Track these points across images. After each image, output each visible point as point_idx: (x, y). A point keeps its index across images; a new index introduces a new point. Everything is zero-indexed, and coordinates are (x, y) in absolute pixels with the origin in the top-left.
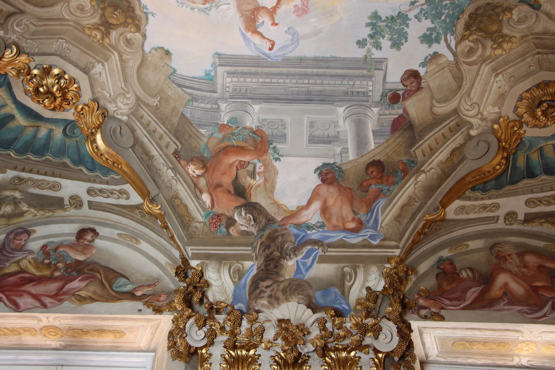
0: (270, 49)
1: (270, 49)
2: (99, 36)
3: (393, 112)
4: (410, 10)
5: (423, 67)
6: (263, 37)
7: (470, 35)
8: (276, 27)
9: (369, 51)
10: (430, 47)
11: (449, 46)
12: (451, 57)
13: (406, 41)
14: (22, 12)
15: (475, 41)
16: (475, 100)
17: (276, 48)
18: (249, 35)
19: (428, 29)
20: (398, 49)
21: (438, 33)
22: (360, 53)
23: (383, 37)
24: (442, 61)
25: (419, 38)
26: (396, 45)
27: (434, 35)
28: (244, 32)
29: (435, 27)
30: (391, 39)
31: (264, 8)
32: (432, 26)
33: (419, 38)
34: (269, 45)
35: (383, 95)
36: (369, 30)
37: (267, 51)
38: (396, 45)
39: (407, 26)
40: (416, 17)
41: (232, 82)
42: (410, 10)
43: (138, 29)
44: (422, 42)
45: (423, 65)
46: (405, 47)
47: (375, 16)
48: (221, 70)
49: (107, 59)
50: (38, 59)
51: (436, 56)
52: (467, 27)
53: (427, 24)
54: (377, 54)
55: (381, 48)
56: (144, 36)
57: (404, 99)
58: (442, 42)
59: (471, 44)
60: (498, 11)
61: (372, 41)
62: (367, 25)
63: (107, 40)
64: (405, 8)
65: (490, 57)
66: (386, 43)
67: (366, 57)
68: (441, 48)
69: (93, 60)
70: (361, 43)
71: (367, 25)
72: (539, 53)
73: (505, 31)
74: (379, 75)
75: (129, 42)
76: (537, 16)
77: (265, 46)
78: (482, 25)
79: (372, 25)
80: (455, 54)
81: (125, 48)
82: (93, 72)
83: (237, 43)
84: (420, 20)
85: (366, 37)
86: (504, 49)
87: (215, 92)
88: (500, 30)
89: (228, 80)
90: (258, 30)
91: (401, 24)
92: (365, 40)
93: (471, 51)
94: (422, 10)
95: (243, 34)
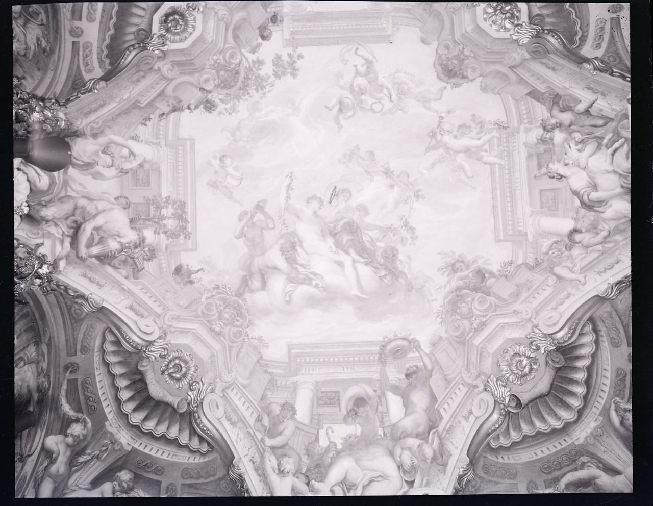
0: (357, 49)
1: (357, 49)
2: (466, 50)
3: (274, 10)
4: (274, 81)
5: (259, 43)
6: (362, 56)
7: (235, 68)
8: (355, 64)
9: (295, 52)
10: (258, 57)
11: (247, 59)
12: (243, 51)
13: (273, 60)
14: (511, 67)
15: (231, 64)
16: (222, 22)
17: (354, 49)
18: (371, 58)
19: (261, 69)
20: (277, 55)
21: (254, 67)
22: (300, 50)
23: (287, 62)
24: (249, 49)
25: (265, 63)
26: (278, 57)
27: (256, 66)
28: (374, 60)
29: (257, 71)
30: (283, 61)
31: (362, 76)
32: (259, 72)
33: (265, 63)
34: (359, 52)
35: (282, 21)
36: (297, 65)
37: (360, 48)
38: (278, 57)
39: (274, 71)
40: (270, 77)
41: (382, 24)
42: (274, 81)
43: (439, 56)
44: (263, 60)
45: (259, 45)
46: (273, 56)
47: (294, 76)
48: (389, 32)
49: (463, 35)
50: (507, 35)
51: (253, 51)
52: (237, 73)
53: (262, 73)
54: (290, 50)
55: (288, 54)
56: (437, 52)
57: (268, 19)
58: (251, 62)
59: (233, 61)
60: (223, 85)
61: (294, 59)
62: (298, 70)
63: (461, 48)
64: (277, 82)
65: (220, 53)
66: (285, 58)
67: (297, 48)
68: (252, 57)
69: (471, 34)
70: (300, 57)
71: (298, 70)
72: (191, 60)
73: (214, 72)
74: (287, 36)
75: (447, 47)
76: (199, 83)
77: (362, 51)
78: (230, 74)
79: (294, 69)
80: (242, 54)
81: (450, 43)
82: (473, 26)
83: (380, 52)
84: (267, 74)
85: (298, 61)
86: (213, 60)
87: (393, 16)
88: (218, 72)
89: (384, 26)
90: (365, 61)
91: (278, 71)
92: (298, 59)
93: (232, 56)
94: (267, 82)
95: (375, 58)
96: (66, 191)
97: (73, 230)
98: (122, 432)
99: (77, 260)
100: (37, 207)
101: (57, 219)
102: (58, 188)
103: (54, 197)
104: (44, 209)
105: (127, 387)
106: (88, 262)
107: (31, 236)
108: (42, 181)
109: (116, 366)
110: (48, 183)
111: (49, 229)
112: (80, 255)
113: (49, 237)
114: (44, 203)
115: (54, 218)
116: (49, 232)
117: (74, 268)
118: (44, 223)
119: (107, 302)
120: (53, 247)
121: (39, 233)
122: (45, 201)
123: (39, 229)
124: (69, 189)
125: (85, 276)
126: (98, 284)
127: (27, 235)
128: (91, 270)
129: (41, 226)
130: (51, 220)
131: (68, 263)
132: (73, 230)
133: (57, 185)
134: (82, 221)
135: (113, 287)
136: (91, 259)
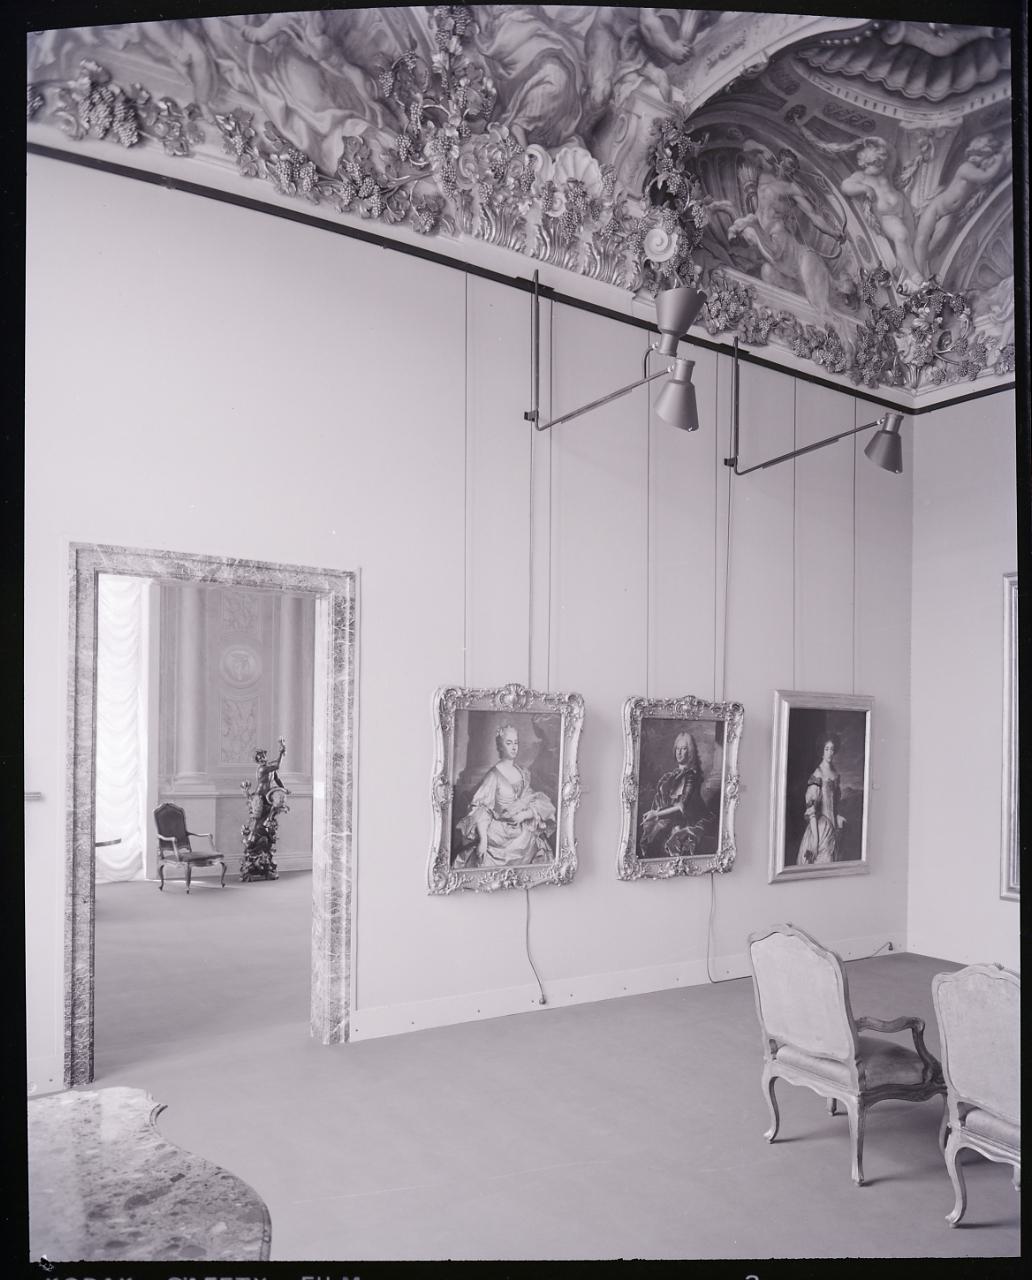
96: (577, 35)
97: (640, 52)
98: (933, 117)
99: (684, 66)
100: (588, 106)
101: (614, 75)
102: (571, 52)
103: (581, 65)
104: (593, 92)
105: (891, 72)
106: (697, 48)
107: (621, 137)
108: (552, 81)
109: (851, 65)
110: (557, 67)
111: (623, 97)
112: (681, 58)
113: (634, 103)
114: (584, 90)
115: (610, 79)
116: (627, 99)
117: (692, 78)
118: (611, 102)
119: (769, 46)
120: (648, 99)
121: (623, 119)
122: (582, 86)
123: (617, 116)
124: (576, 28)
125: (712, 64)
126: (737, 46)
127: (621, 141)
128: (711, 49)
129: (614, 110)
130: (613, 85)
131: (681, 84)
132: (640, 52)
133: (565, 51)
134: (634, 27)
135: (757, 22)
136: (696, 41)
